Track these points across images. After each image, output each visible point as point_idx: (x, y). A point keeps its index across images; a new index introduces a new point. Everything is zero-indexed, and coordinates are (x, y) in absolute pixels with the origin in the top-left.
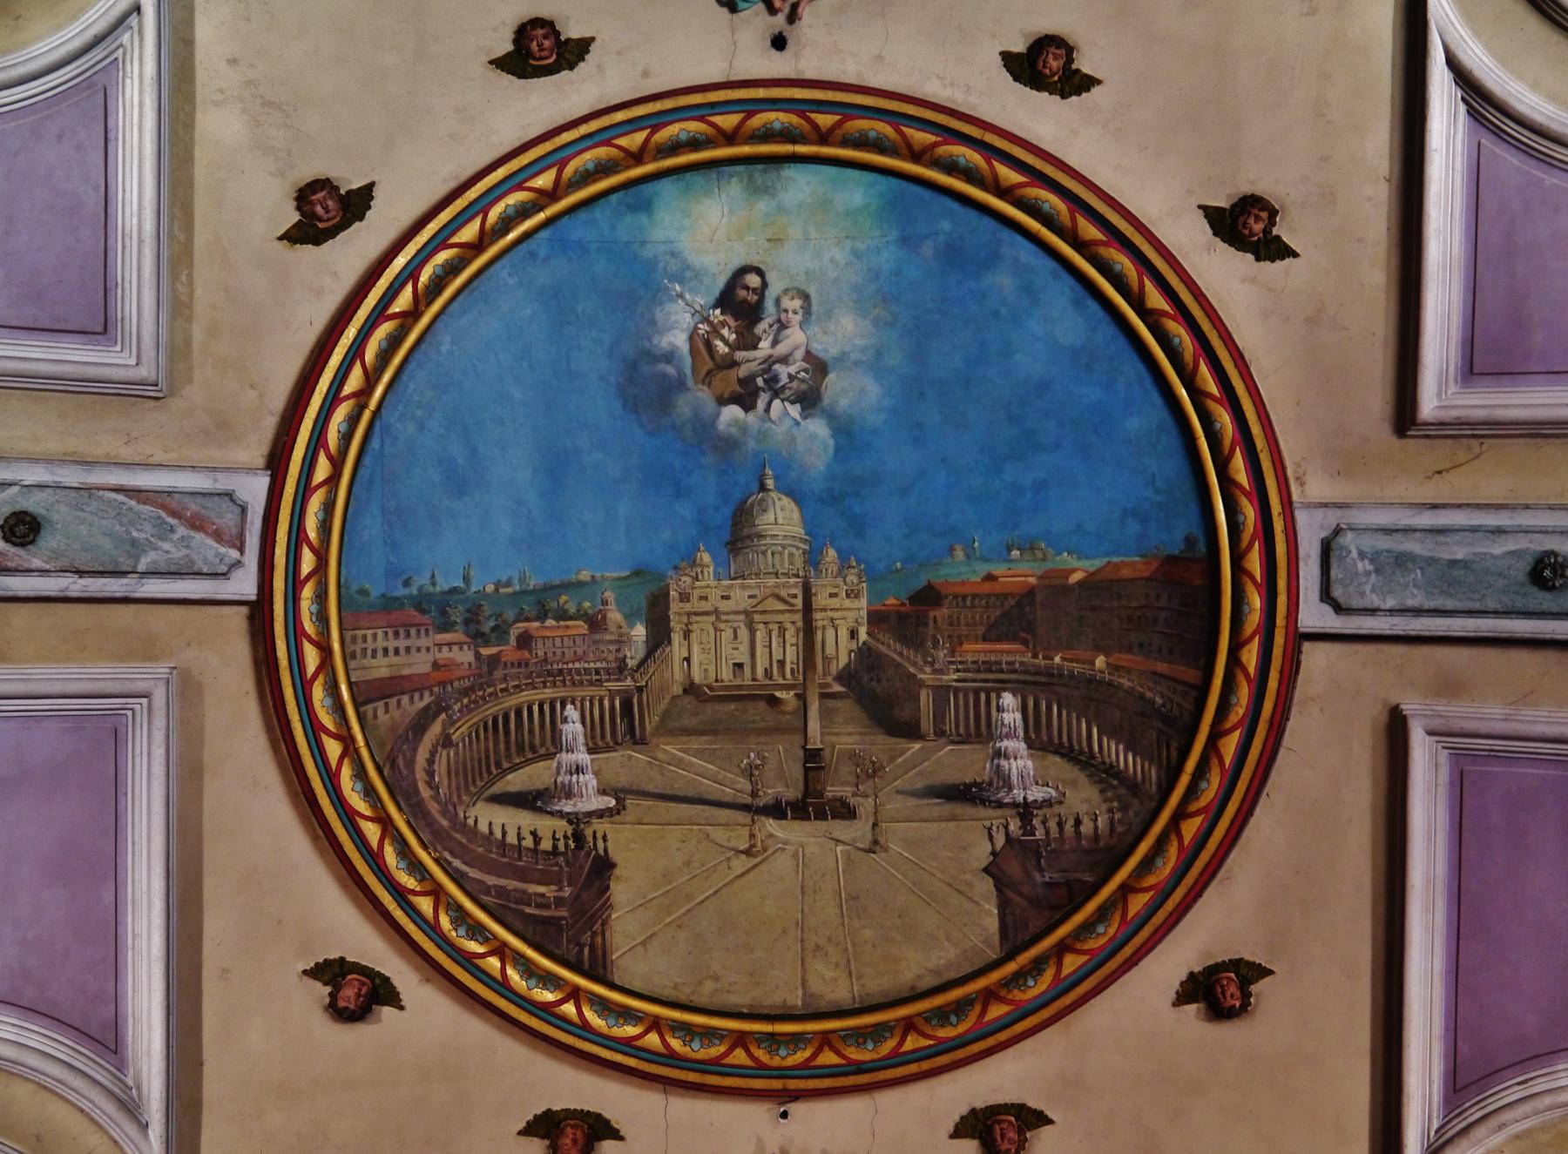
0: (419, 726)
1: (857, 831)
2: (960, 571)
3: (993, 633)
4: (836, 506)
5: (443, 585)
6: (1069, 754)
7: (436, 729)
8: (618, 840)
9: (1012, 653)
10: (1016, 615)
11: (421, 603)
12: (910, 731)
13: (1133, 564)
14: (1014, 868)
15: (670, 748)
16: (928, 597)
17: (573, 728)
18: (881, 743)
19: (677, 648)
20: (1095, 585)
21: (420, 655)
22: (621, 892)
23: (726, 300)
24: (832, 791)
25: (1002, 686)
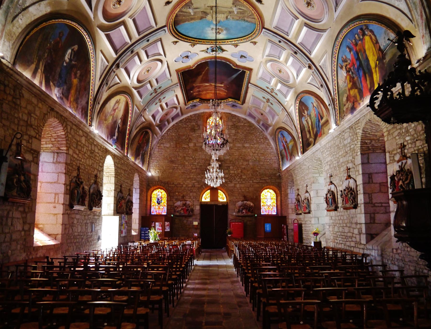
0: (250, 16)
1: (206, 5)
2: (198, 21)
3: (195, 18)
4: (210, 23)
5: (247, 23)
6: (186, 12)
7: (249, 15)
8: (232, 5)
9: (193, 17)
10: (192, 19)
11: (249, 22)
12: (202, 12)
13: (182, 24)
14: (190, 5)
15: (226, 10)
16: (201, 19)
17: (236, 13)
18: (205, 11)
19: (225, 16)
20: (185, 22)
21: (249, 19)
22: (232, 2)
23: (220, 33)
24: (210, 8)
25: (193, 15)
